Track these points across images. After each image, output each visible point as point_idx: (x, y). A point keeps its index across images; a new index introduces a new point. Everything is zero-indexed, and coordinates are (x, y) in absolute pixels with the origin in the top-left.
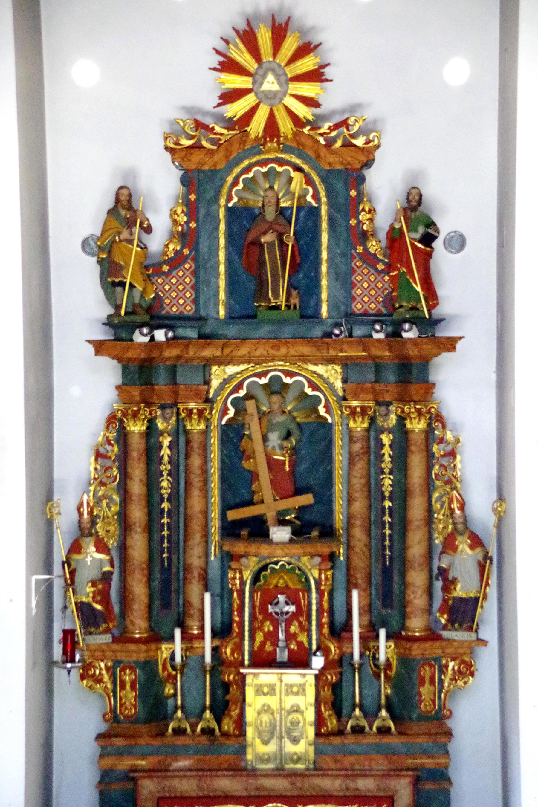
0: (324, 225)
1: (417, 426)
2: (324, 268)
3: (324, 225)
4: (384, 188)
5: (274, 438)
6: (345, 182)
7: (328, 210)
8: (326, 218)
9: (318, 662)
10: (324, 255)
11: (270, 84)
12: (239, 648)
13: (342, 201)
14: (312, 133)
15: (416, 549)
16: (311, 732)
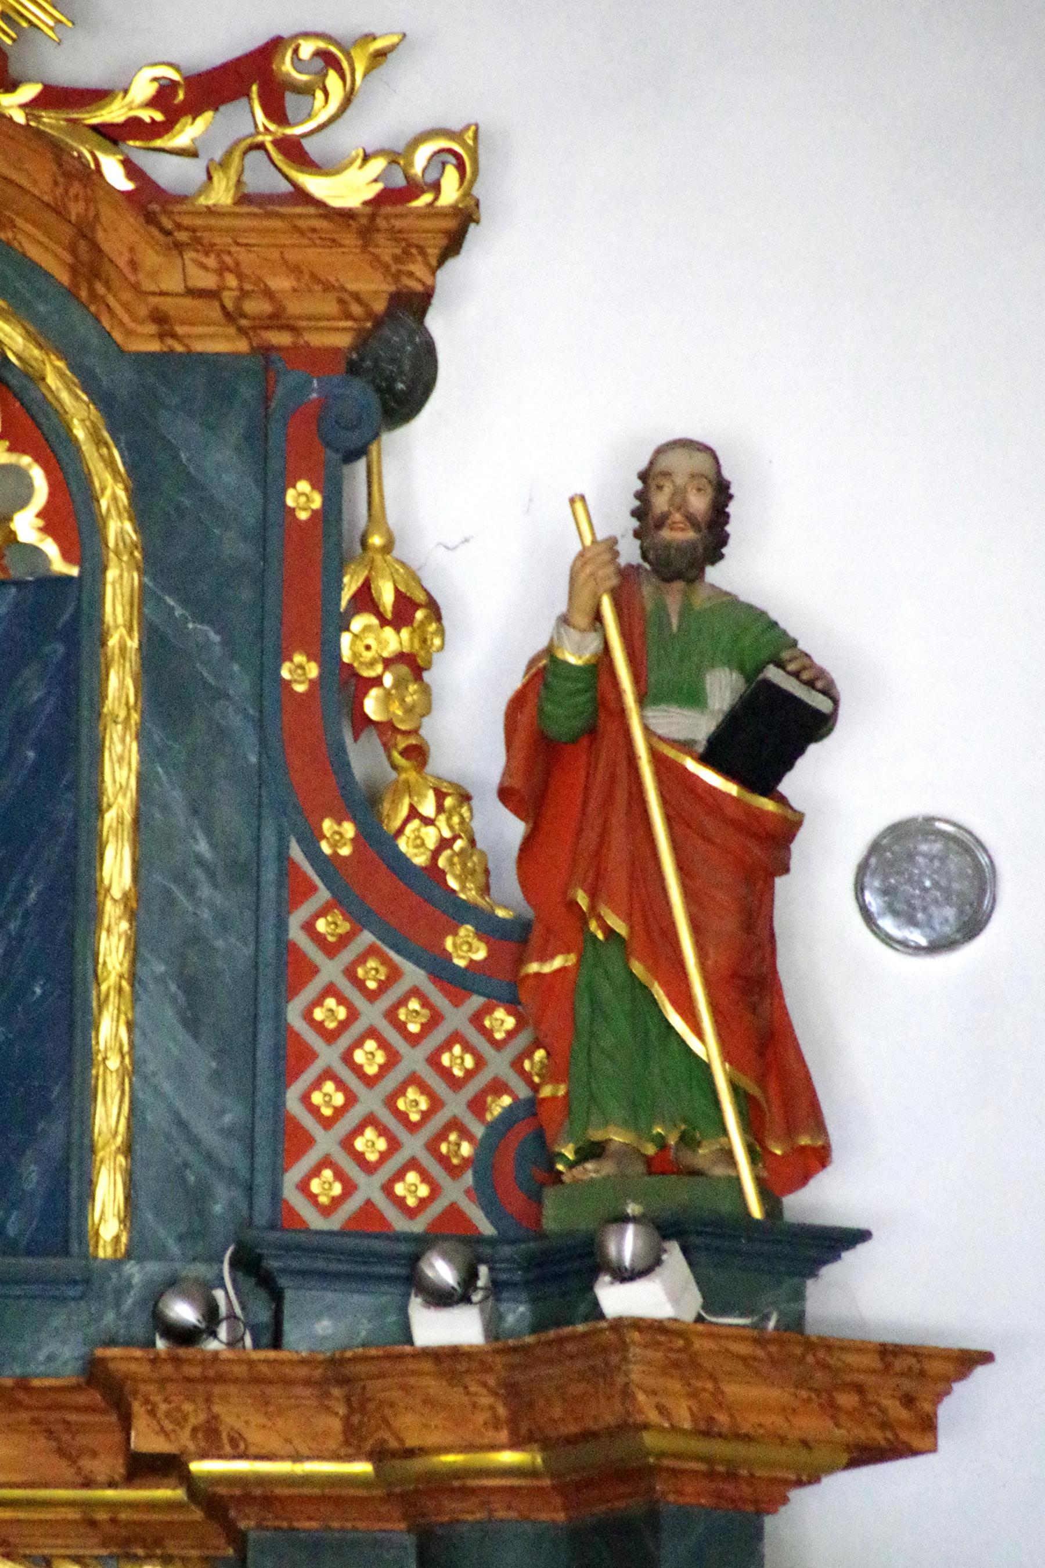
0: (120, 687)
2: (112, 951)
3: (120, 687)
6: (256, 438)
7: (145, 599)
8: (133, 644)
10: (117, 869)
13: (233, 547)
14: (49, 120)
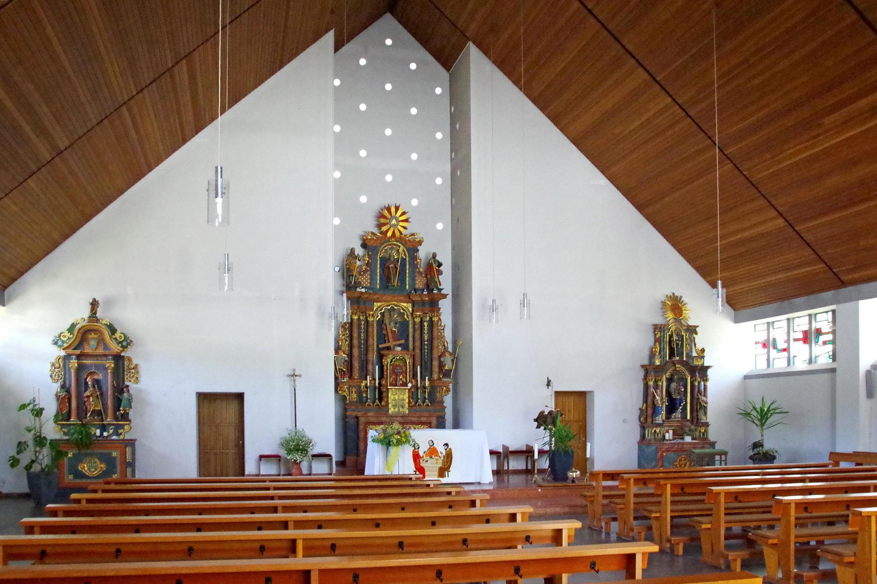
1: (435, 319)
4: (423, 253)
5: (392, 324)
9: (410, 385)
11: (394, 222)
12: (386, 382)
15: (436, 354)
16: (407, 406)
